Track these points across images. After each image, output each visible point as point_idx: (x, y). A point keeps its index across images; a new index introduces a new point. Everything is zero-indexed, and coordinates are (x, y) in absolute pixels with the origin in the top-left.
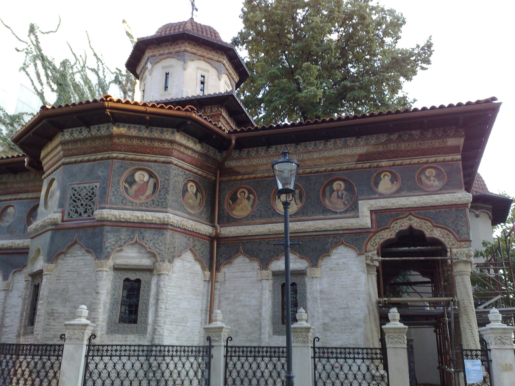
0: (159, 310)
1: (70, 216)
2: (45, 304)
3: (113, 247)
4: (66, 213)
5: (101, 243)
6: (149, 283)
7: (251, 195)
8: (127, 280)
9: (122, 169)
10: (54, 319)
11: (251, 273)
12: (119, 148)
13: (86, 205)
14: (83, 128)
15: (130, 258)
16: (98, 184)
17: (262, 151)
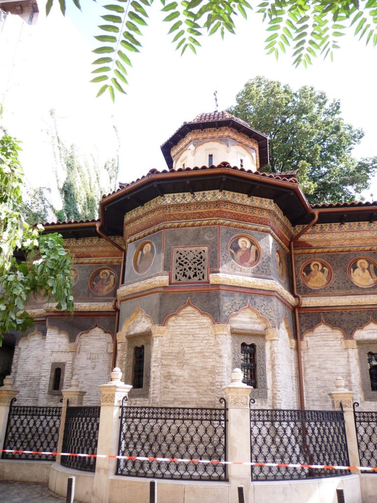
0: (277, 375)
1: (178, 279)
2: (160, 367)
3: (230, 311)
4: (173, 275)
5: (219, 306)
6: (263, 348)
7: (324, 268)
8: (243, 345)
9: (228, 235)
10: (172, 382)
11: (335, 342)
12: (225, 215)
13: (195, 269)
14: (186, 194)
15: (244, 322)
16: (206, 249)
17: (336, 226)
